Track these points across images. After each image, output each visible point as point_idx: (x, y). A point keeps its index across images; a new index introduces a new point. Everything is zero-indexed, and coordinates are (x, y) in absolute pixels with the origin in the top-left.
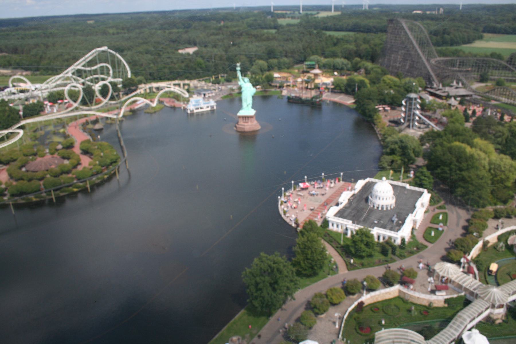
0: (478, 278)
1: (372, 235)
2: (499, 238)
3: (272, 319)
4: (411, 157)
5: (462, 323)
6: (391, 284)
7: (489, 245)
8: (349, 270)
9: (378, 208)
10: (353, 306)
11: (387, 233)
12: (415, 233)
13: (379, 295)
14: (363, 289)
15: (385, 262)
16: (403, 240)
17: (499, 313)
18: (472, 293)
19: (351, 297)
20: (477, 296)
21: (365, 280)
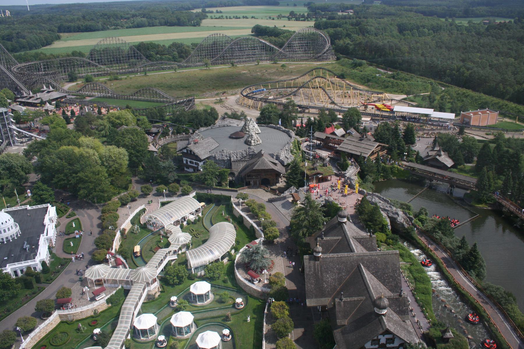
0: (127, 266)
1: (6, 273)
2: (133, 222)
5: (129, 313)
6: (49, 314)
7: (126, 232)
11: (24, 264)
12: (54, 251)
13: (40, 332)
14: (19, 335)
15: (34, 295)
16: (43, 263)
17: (155, 287)
18: (127, 283)
20: (132, 283)
21: (17, 325)
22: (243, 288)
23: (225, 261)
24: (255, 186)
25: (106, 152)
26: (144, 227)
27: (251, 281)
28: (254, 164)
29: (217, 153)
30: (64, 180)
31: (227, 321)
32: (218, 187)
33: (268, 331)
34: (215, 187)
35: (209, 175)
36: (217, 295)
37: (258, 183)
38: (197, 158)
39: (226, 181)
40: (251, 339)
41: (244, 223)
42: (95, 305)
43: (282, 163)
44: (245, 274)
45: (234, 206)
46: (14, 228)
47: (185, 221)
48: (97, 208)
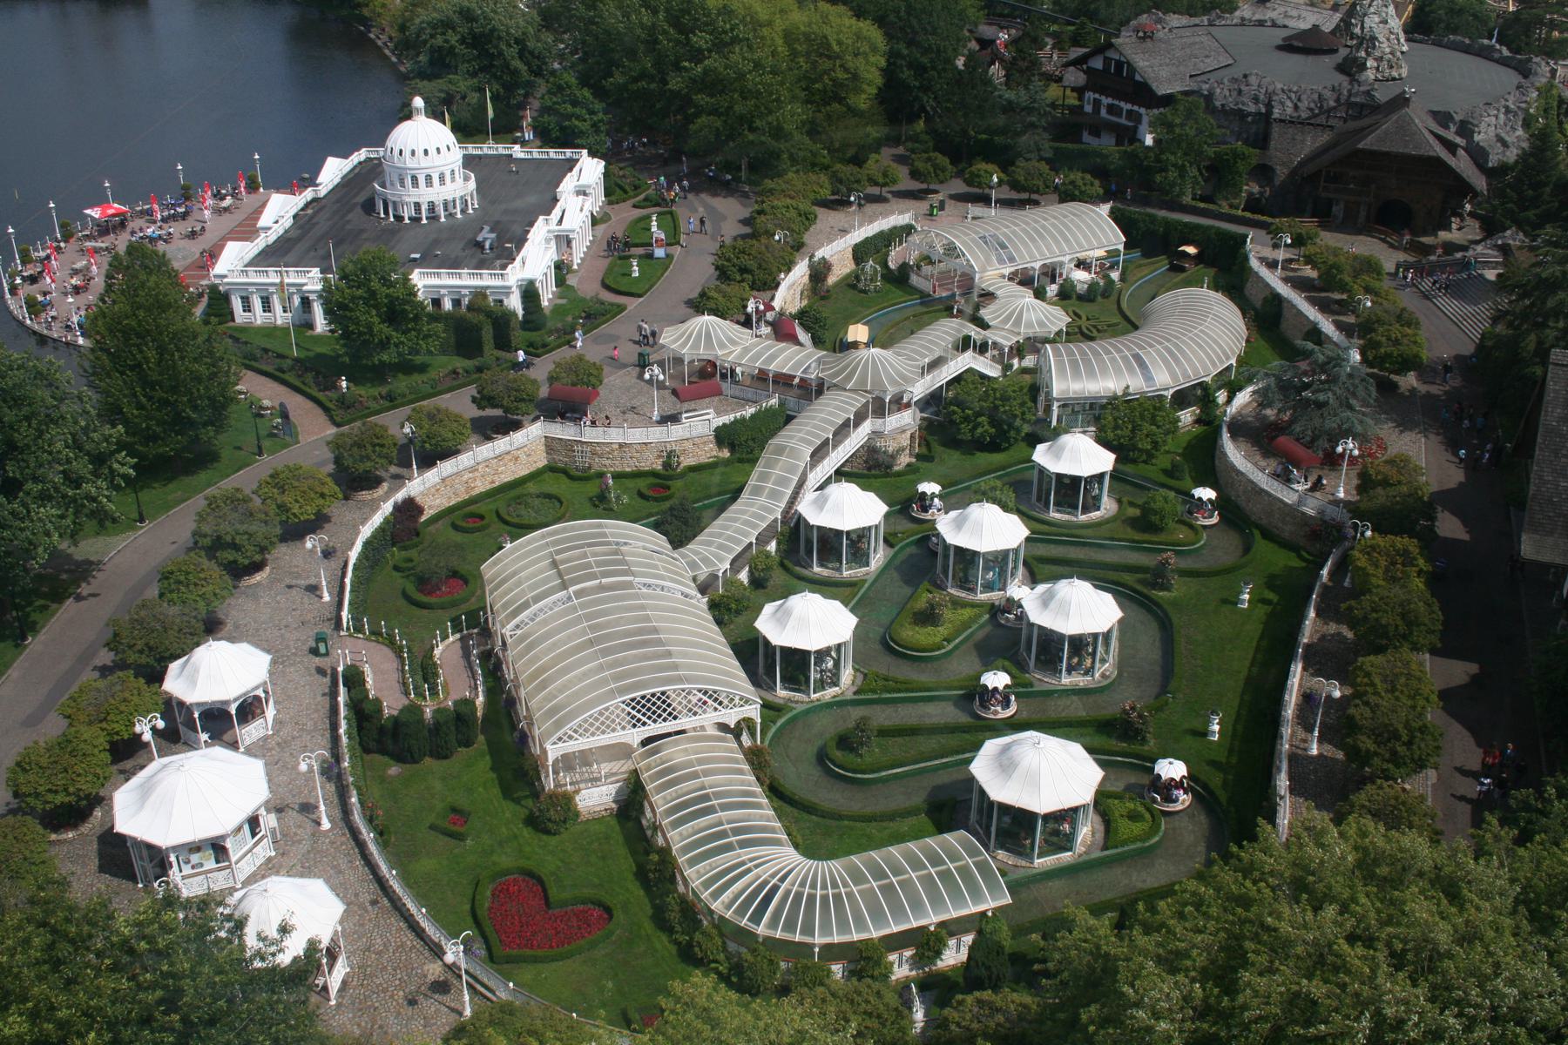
2: (860, 252)
3: (35, 644)
4: (515, 73)
6: (508, 426)
7: (832, 280)
8: (338, 425)
9: (416, 220)
10: (377, 520)
11: (466, 280)
12: (572, 281)
13: (472, 469)
16: (530, 293)
19: (365, 495)
22: (1242, 502)
23: (1187, 416)
24: (1349, 226)
25: (810, 25)
26: (899, 278)
27: (1285, 478)
28: (1362, 132)
29: (1220, 83)
30: (652, 78)
31: (1154, 586)
32: (1202, 205)
33: (1323, 638)
34: (1187, 199)
35: (1173, 153)
36: (1131, 504)
37: (1363, 214)
38: (1142, 93)
39: (1237, 195)
40: (1240, 661)
41: (1284, 326)
42: (676, 432)
43: (1478, 155)
44: (1258, 457)
45: (1254, 263)
46: (459, 180)
47: (1053, 281)
48: (745, 195)
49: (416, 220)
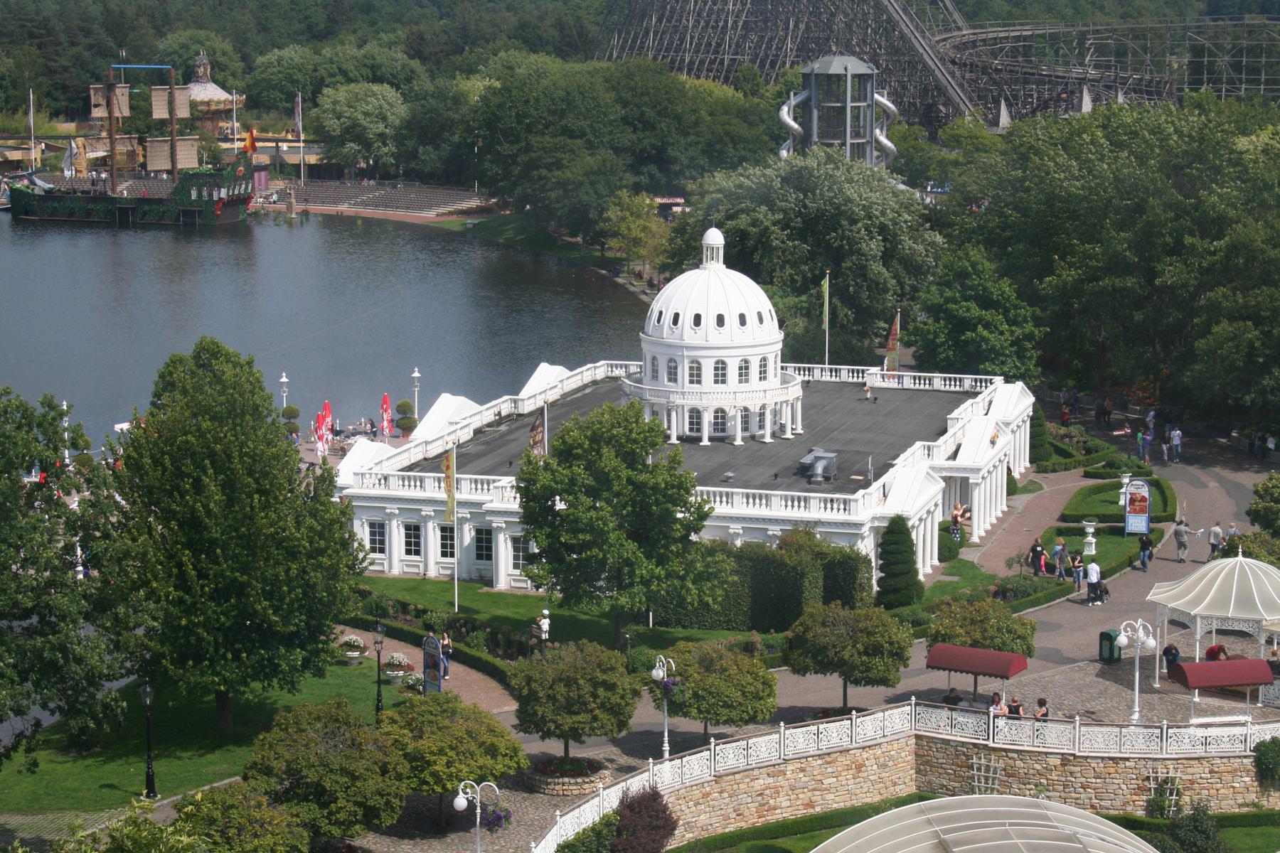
11: (780, 509)
13: (775, 769)
46: (773, 380)
49: (691, 440)
